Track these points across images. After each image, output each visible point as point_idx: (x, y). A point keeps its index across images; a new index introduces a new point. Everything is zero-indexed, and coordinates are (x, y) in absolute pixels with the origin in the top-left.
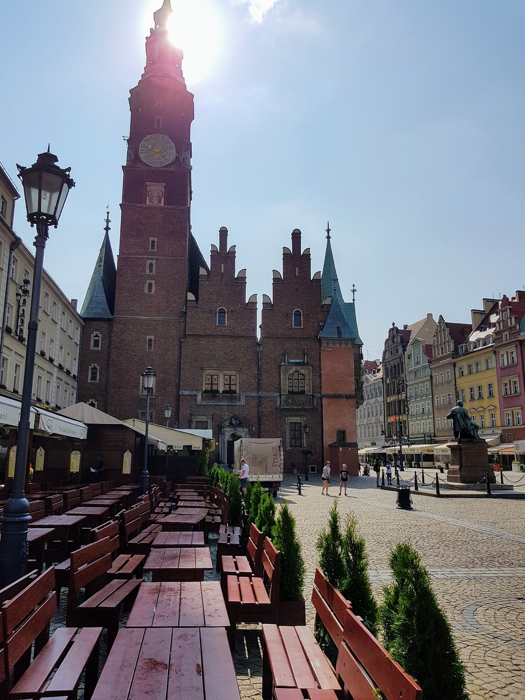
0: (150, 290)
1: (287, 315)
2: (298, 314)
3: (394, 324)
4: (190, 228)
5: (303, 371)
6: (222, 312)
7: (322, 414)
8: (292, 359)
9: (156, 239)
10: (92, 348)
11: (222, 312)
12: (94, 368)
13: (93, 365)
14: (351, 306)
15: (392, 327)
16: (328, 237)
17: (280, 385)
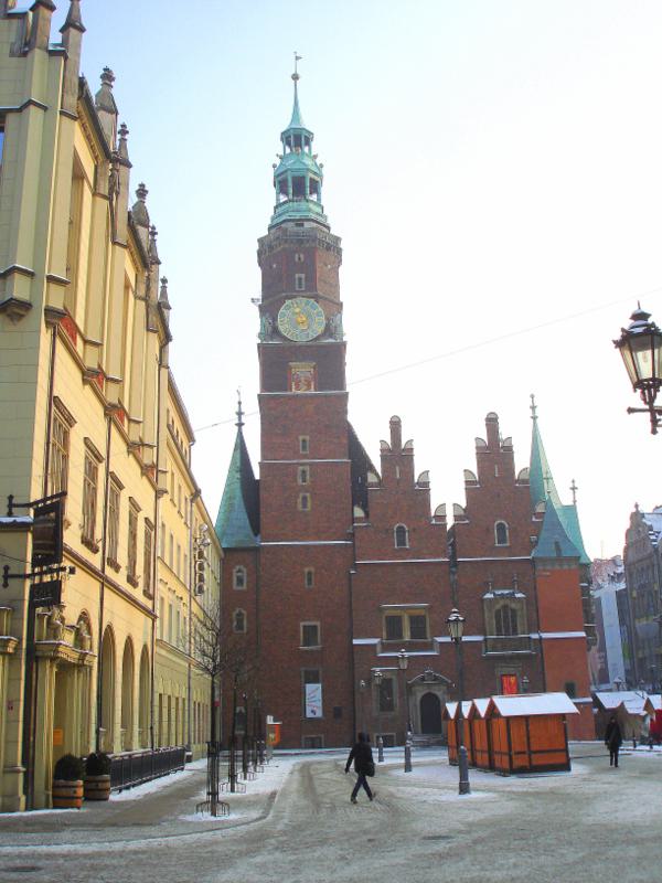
0: (305, 506)
1: (488, 530)
2: (501, 527)
3: (637, 506)
4: (346, 412)
5: (513, 606)
6: (401, 530)
7: (543, 662)
8: (499, 589)
9: (308, 438)
10: (235, 587)
11: (401, 530)
12: (240, 614)
13: (237, 611)
14: (571, 510)
15: (634, 510)
16: (534, 418)
17: (484, 624)
